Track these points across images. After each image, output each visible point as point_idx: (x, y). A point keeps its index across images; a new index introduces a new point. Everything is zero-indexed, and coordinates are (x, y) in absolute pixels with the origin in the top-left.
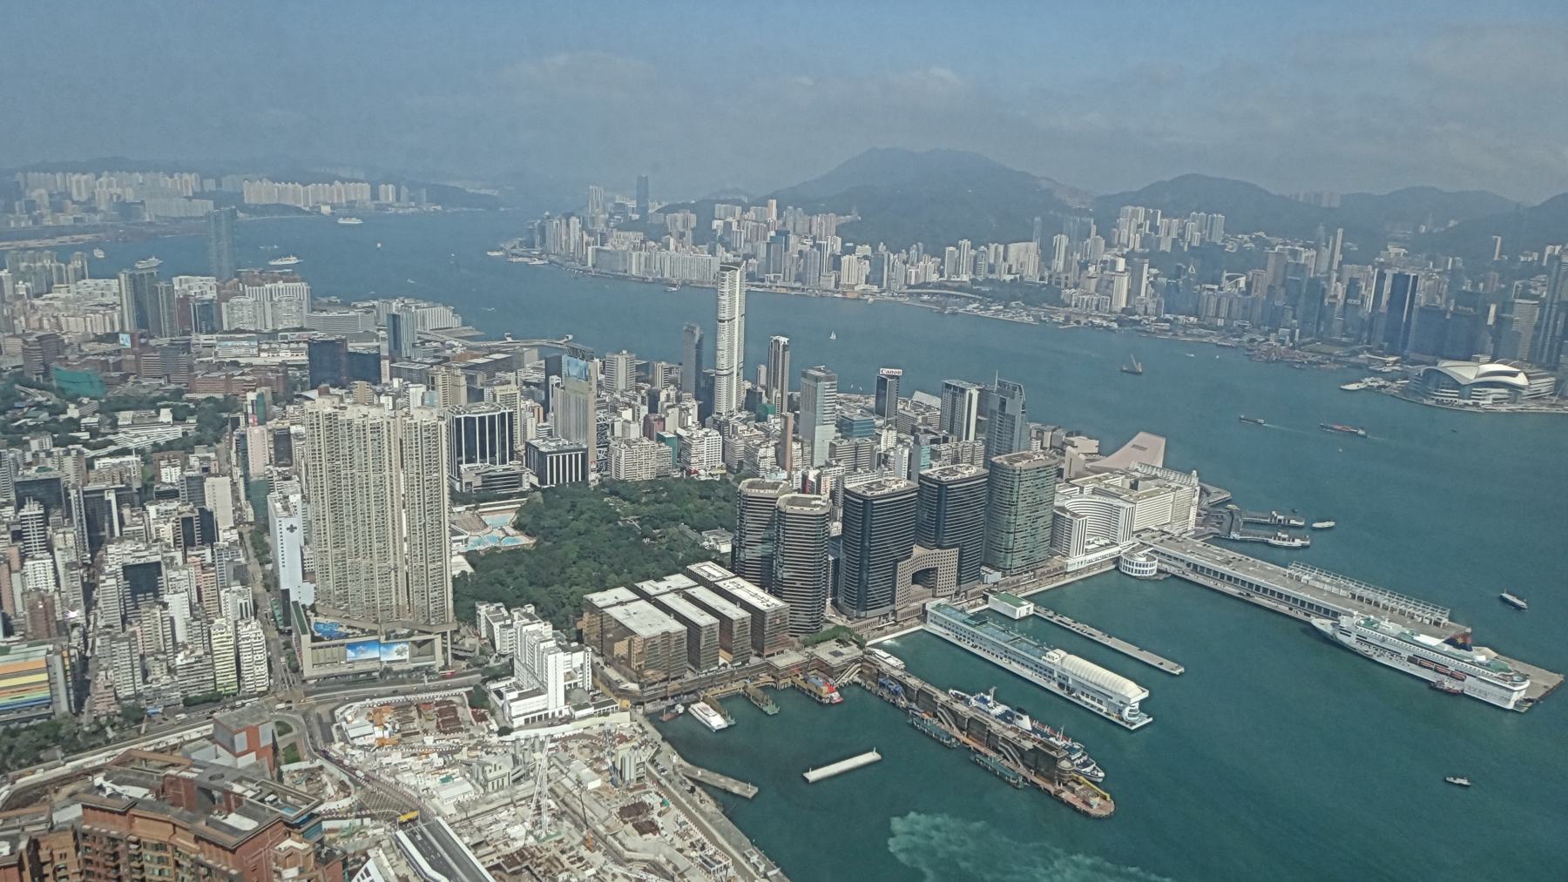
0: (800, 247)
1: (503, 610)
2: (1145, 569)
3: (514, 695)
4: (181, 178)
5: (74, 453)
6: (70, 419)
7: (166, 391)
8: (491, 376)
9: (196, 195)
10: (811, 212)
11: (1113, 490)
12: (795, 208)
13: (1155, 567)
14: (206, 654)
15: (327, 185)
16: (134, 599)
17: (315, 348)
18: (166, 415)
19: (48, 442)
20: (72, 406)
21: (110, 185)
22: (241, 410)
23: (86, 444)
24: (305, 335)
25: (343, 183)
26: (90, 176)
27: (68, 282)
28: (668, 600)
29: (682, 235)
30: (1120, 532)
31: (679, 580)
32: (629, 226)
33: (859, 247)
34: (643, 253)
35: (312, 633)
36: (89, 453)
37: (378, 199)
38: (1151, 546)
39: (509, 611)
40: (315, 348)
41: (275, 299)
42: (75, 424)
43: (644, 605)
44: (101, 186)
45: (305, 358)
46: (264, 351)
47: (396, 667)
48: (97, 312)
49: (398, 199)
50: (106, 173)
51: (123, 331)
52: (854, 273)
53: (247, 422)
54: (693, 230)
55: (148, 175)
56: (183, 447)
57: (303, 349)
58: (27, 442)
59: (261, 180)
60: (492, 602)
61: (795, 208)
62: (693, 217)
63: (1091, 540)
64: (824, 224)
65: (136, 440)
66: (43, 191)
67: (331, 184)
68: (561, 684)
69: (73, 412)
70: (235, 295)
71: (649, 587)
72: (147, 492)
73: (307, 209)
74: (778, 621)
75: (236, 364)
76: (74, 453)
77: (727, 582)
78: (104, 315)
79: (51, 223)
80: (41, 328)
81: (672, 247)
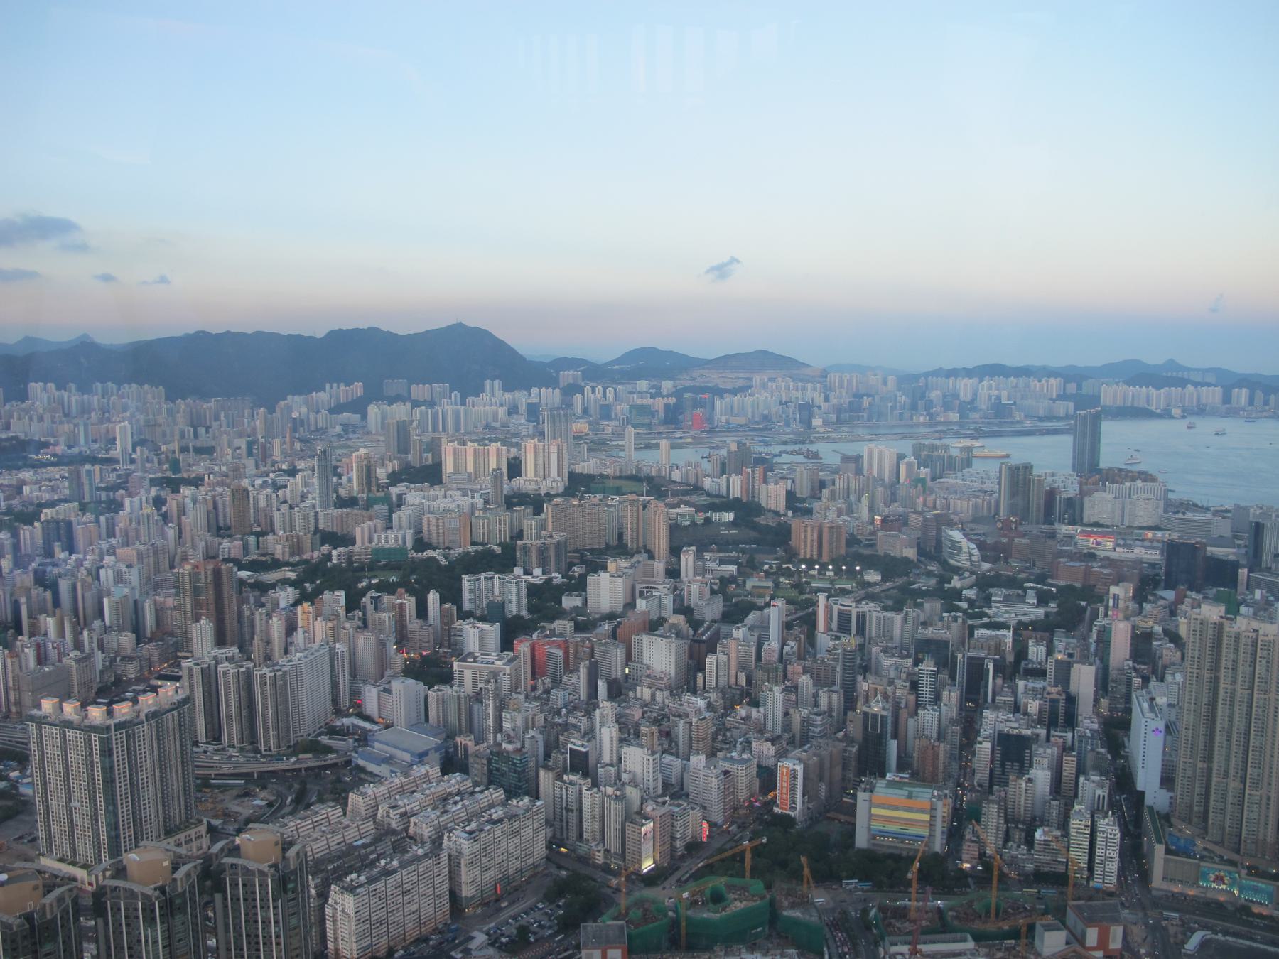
4: (1047, 381)
5: (960, 620)
6: (954, 588)
7: (1032, 574)
9: (1062, 397)
14: (1062, 836)
17: (1172, 549)
18: (1031, 599)
20: (956, 577)
21: (990, 388)
22: (1101, 601)
24: (1159, 534)
25: (1196, 387)
26: (975, 381)
27: (955, 469)
36: (970, 622)
40: (1172, 549)
41: (1135, 497)
42: (957, 594)
44: (983, 389)
45: (1158, 557)
46: (1119, 545)
48: (978, 497)
49: (1251, 402)
51: (997, 513)
53: (1106, 615)
55: (1021, 379)
56: (1046, 628)
57: (1157, 548)
58: (921, 605)
59: (1117, 384)
65: (1006, 616)
66: (938, 392)
67: (1184, 387)
69: (956, 583)
70: (1097, 491)
72: (1016, 667)
73: (1158, 411)
75: (1092, 556)
76: (960, 620)
78: (983, 500)
80: (934, 508)
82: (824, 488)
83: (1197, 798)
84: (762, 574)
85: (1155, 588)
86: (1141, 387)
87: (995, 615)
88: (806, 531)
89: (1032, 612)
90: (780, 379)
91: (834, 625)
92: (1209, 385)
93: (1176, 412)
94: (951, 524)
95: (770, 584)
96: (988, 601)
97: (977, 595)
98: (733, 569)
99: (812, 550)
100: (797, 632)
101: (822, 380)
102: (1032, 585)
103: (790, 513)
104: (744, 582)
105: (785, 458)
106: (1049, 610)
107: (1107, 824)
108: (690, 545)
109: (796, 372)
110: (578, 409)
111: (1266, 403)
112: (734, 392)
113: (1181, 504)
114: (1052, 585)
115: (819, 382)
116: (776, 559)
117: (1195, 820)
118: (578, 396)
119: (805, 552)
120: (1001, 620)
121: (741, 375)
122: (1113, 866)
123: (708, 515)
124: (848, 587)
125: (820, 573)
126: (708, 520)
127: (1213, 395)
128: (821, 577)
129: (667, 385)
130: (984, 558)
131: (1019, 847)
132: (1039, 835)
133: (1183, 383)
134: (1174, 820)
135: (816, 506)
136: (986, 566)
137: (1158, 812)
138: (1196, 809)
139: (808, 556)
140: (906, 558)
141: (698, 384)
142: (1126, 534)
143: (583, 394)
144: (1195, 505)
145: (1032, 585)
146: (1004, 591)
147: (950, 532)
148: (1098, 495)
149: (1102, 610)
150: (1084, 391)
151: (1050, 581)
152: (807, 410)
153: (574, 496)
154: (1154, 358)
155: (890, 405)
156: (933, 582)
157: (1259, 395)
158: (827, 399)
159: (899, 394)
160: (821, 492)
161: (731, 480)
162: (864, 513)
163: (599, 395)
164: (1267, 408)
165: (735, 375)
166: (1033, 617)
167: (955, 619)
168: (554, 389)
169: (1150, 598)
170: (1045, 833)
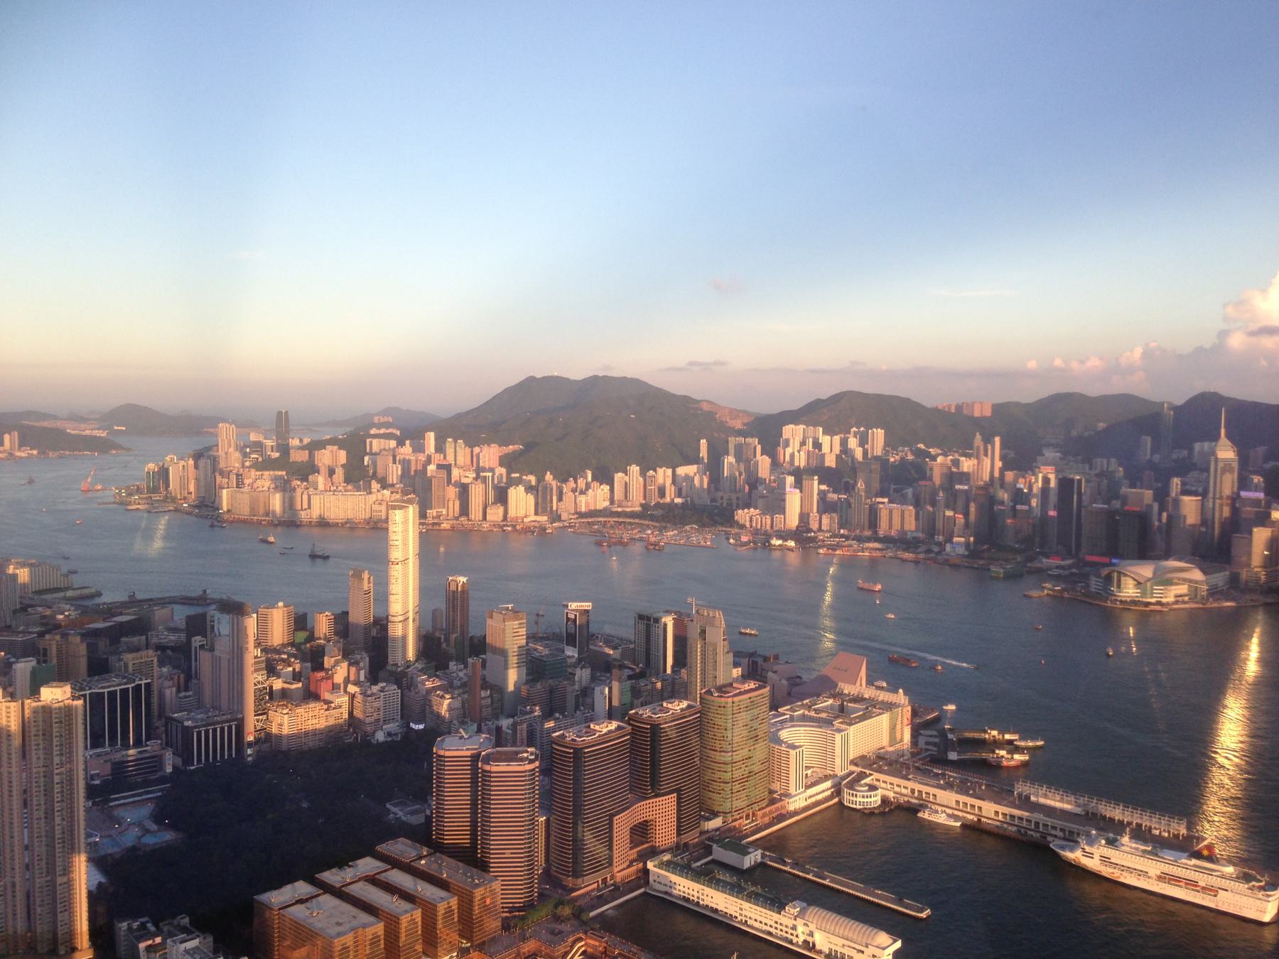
0: (464, 481)
1: (151, 927)
2: (869, 800)
11: (824, 715)
12: (456, 442)
13: (878, 799)
28: (360, 890)
29: (331, 472)
30: (838, 761)
31: (367, 865)
33: (524, 477)
34: (287, 495)
38: (871, 775)
43: (328, 901)
54: (342, 466)
61: (456, 442)
63: (809, 772)
64: (490, 455)
71: (331, 877)
77: (423, 862)
81: (321, 487)
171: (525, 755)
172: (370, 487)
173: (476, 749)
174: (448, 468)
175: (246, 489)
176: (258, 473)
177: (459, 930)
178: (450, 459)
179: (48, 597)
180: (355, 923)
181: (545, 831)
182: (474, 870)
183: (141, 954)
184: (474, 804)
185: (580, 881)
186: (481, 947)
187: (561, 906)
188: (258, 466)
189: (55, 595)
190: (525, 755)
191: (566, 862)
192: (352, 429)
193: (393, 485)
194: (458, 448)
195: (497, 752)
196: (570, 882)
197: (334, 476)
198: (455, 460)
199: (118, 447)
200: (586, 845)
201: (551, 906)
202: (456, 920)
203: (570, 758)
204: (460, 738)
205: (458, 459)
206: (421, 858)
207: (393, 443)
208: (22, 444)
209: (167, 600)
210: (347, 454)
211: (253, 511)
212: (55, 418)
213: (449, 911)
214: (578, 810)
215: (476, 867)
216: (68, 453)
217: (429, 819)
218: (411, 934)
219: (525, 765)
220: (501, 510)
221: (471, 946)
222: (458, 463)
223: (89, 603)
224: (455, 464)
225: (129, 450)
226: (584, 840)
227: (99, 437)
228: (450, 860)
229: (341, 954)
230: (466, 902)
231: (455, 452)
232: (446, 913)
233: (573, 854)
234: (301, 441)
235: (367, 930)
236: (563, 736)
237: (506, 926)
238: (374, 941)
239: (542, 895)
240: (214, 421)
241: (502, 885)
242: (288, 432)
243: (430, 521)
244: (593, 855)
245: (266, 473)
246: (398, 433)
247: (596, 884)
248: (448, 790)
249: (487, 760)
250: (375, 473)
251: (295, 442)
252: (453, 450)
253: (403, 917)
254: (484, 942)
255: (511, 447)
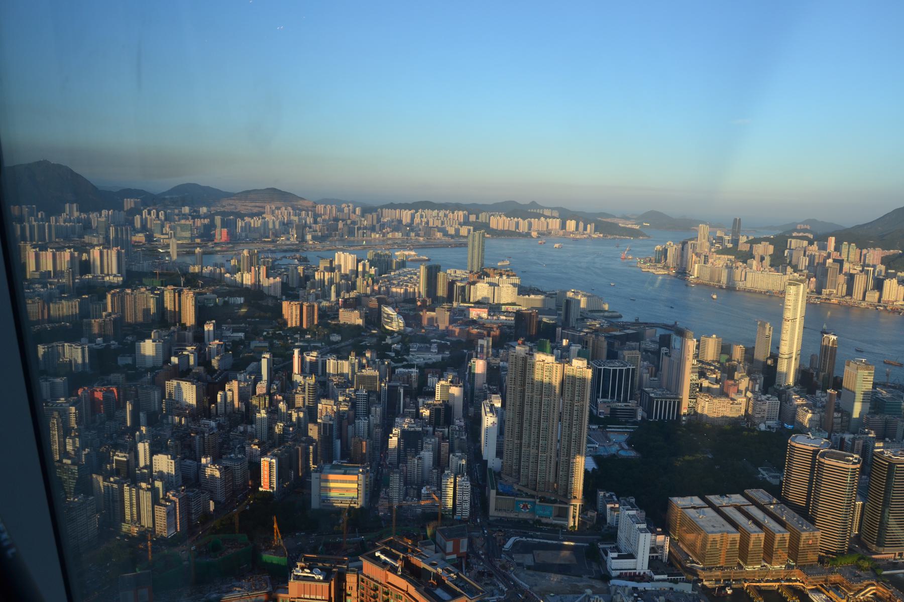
1: (614, 497)
3: (615, 555)
6: (387, 344)
8: (623, 343)
10: (861, 246)
12: (849, 244)
14: (437, 490)
15: (537, 220)
16: (405, 450)
18: (434, 349)
19: (375, 355)
20: (388, 337)
21: (422, 216)
22: (474, 349)
23: (392, 359)
25: (546, 219)
26: (413, 211)
29: (762, 259)
31: (737, 499)
32: (725, 251)
33: (899, 274)
35: (497, 490)
37: (565, 229)
39: (618, 498)
42: (388, 347)
47: (544, 520)
49: (577, 228)
50: (420, 211)
52: (894, 292)
54: (770, 255)
60: (608, 491)
61: (849, 244)
62: (771, 249)
65: (417, 360)
67: (539, 219)
68: (647, 555)
69: (389, 340)
71: (714, 499)
74: (811, 542)
77: (772, 507)
79: (391, 236)
81: (754, 267)
82: (309, 280)
83: (515, 461)
84: (262, 338)
85: (509, 341)
86: (514, 218)
87: (411, 360)
88: (292, 309)
89: (434, 356)
90: (284, 208)
91: (307, 370)
92: (554, 218)
93: (534, 234)
94: (388, 304)
95: (267, 344)
96: (407, 351)
97: (401, 347)
98: (242, 335)
99: (296, 322)
100: (280, 375)
101: (313, 209)
102: (435, 340)
103: (284, 297)
104: (249, 343)
105: (284, 261)
106: (445, 356)
107: (463, 481)
108: (211, 320)
109: (295, 203)
110: (138, 224)
111: (585, 229)
112: (252, 215)
113: (530, 290)
114: (448, 341)
115: (311, 211)
116: (272, 328)
117: (514, 474)
118: (138, 217)
119: (292, 323)
120: (415, 363)
121: (257, 204)
122: (467, 505)
123: (226, 299)
124: (319, 345)
125: (301, 337)
126: (226, 303)
127: (555, 224)
128: (302, 339)
129: (204, 210)
130: (407, 324)
131: (412, 499)
132: (424, 491)
133: (538, 216)
134: (503, 476)
135: (301, 292)
136: (409, 329)
137: (494, 472)
138: (514, 467)
139: (294, 325)
140: (359, 325)
141: (226, 210)
142: (495, 309)
143: (142, 215)
144: (538, 290)
145: (435, 340)
146: (418, 345)
147: (386, 309)
148: (478, 285)
149: (474, 354)
150: (480, 220)
151: (447, 338)
152: (302, 228)
153: (128, 288)
154: (523, 199)
155: (356, 227)
156: (374, 340)
157: (581, 225)
158: (315, 222)
159: (363, 219)
160: (306, 283)
161: (244, 275)
162: (333, 297)
163: (153, 216)
164: (585, 232)
165: (253, 204)
166: (434, 360)
167: (383, 363)
168: (120, 211)
169: (506, 346)
170: (427, 489)
171: (851, 458)
172: (786, 271)
173: (817, 447)
174: (841, 262)
175: (709, 265)
176: (717, 256)
177: (789, 553)
178: (844, 257)
179: (595, 314)
180: (723, 529)
181: (861, 511)
182: (805, 521)
183: (608, 510)
184: (811, 482)
185: (881, 549)
186: (801, 568)
187: (862, 560)
188: (719, 252)
189: (598, 314)
190: (851, 458)
191: (873, 534)
192: (782, 232)
193: (802, 271)
194: (850, 249)
195: (832, 452)
196: (874, 547)
197: (764, 262)
198: (848, 257)
199: (643, 235)
200: (890, 527)
201: (855, 559)
202: (787, 546)
203: (885, 468)
204: (808, 438)
205: (850, 256)
206: (771, 504)
207: (805, 243)
208: (595, 231)
209: (655, 325)
210: (774, 247)
211: (711, 279)
212: (614, 217)
213: (783, 540)
214: (886, 503)
215: (807, 519)
216: (618, 237)
217: (781, 482)
218: (756, 546)
219: (851, 463)
220: (877, 294)
221: (796, 565)
222: (850, 259)
223: (614, 320)
224: (848, 260)
225: (649, 237)
226: (889, 524)
227: (635, 229)
228: (790, 510)
229: (712, 544)
230: (795, 539)
231: (849, 251)
232: (781, 540)
233: (879, 531)
234: (748, 238)
235: (729, 535)
236: (882, 453)
237: (821, 560)
238: (733, 542)
239: (851, 551)
240: (697, 222)
241: (822, 535)
242: (739, 232)
243: (824, 296)
244: (894, 535)
245: (723, 256)
246: (811, 236)
247: (893, 555)
248: (795, 469)
249: (823, 455)
250: (790, 262)
251: (743, 239)
252: (847, 250)
253: (752, 534)
254: (805, 565)
255: (892, 251)
